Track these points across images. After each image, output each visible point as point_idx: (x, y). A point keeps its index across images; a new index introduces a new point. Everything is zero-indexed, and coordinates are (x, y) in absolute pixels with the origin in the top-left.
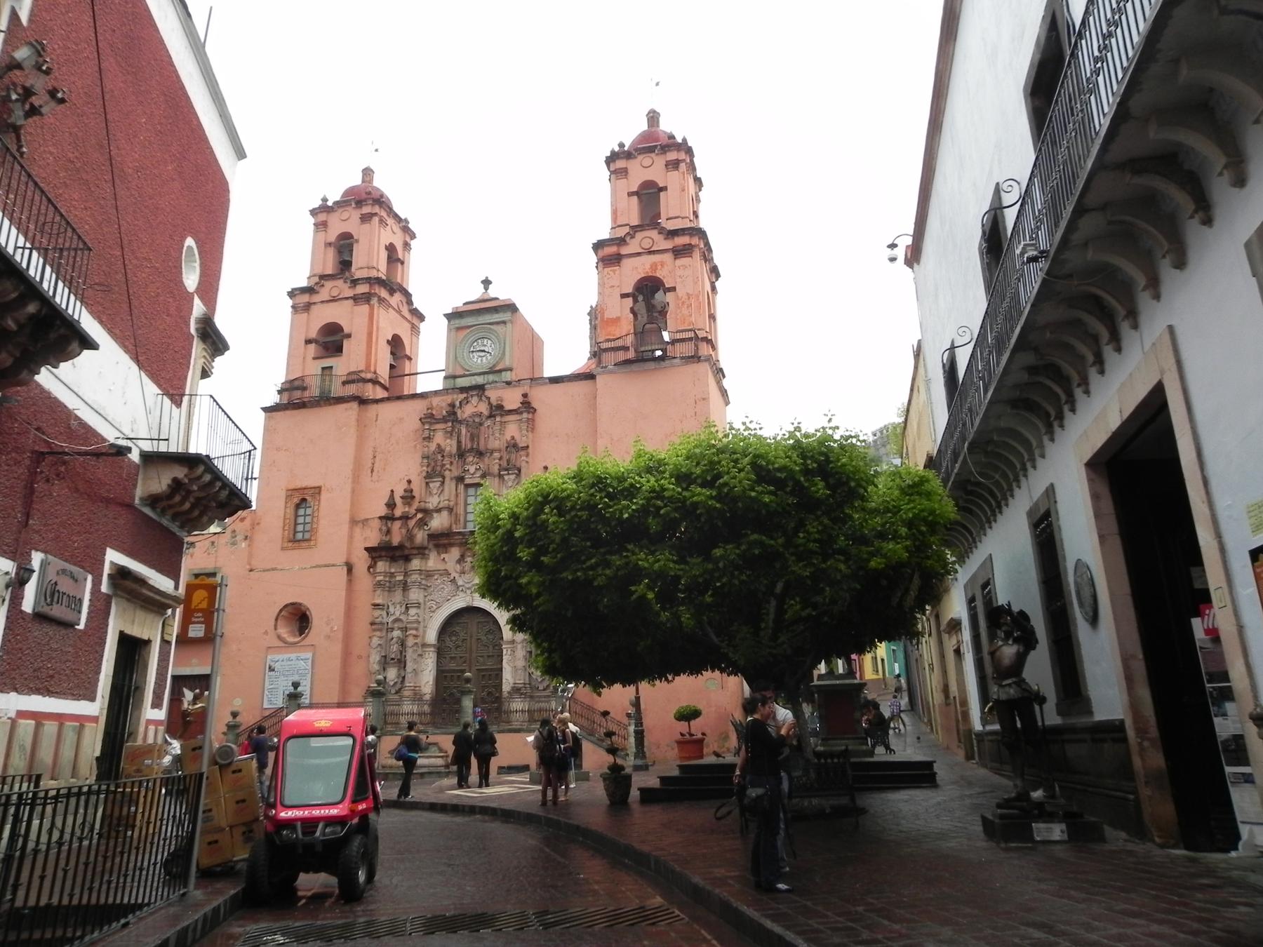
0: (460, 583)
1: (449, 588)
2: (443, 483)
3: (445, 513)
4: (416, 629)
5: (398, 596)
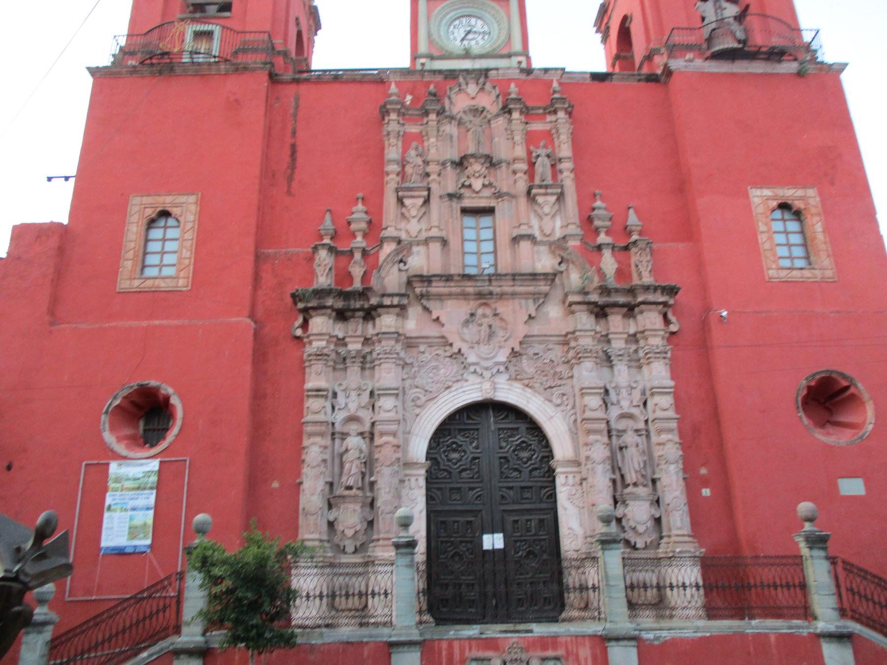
0: (472, 358)
1: (448, 369)
2: (427, 201)
3: (435, 247)
4: (394, 434)
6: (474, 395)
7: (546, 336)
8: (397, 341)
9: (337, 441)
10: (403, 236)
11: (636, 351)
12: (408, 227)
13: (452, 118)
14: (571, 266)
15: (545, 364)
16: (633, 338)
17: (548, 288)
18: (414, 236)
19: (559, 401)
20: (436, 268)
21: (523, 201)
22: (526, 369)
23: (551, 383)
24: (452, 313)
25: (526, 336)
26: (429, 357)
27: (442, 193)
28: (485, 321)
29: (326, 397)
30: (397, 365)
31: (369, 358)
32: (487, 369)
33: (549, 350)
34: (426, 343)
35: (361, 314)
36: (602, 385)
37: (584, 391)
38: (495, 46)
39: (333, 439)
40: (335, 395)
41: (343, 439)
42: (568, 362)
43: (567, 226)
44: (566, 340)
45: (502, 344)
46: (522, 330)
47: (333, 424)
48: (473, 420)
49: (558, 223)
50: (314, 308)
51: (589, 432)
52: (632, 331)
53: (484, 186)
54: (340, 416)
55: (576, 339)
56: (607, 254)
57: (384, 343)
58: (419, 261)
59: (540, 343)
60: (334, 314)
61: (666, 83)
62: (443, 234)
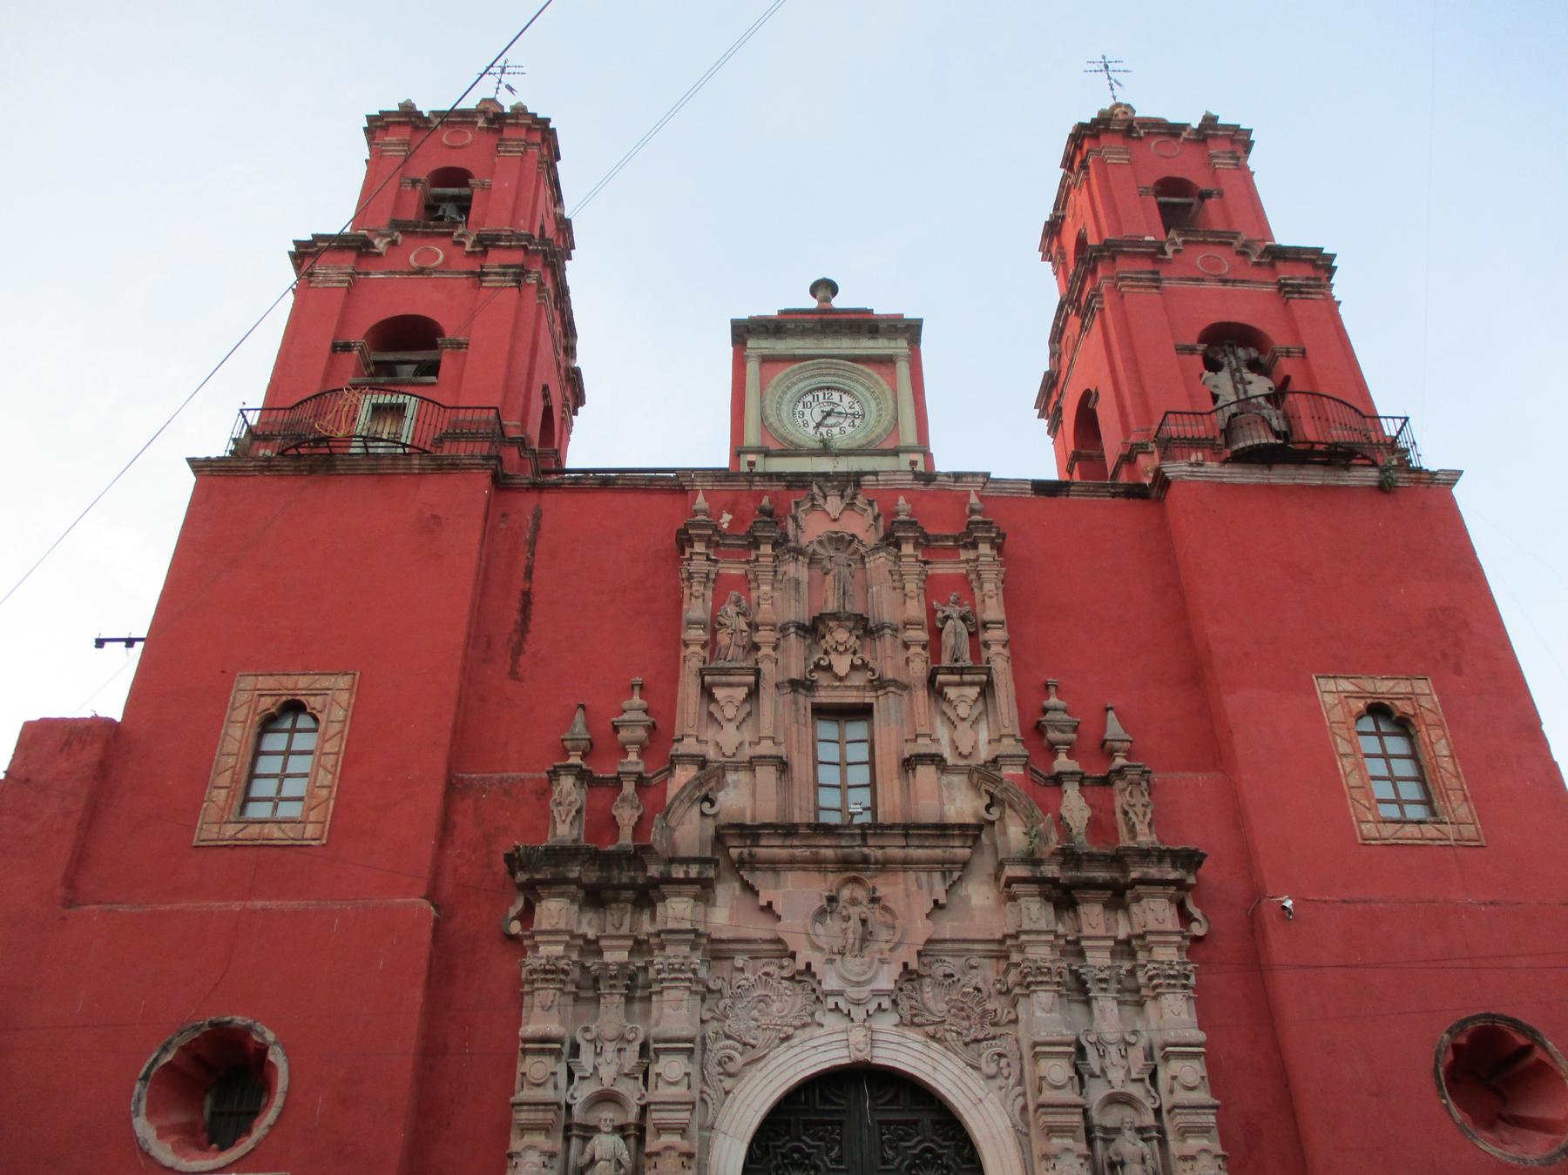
0: (831, 982)
1: (787, 1003)
2: (753, 693)
3: (767, 774)
4: (683, 1131)
5: (611, 1015)
6: (835, 1054)
7: (965, 941)
8: (694, 946)
9: (575, 1142)
10: (711, 753)
11: (1132, 973)
12: (720, 737)
13: (799, 552)
14: (1008, 811)
15: (965, 994)
16: (1125, 948)
17: (968, 851)
18: (729, 753)
19: (992, 1069)
20: (768, 811)
21: (921, 694)
22: (931, 1005)
23: (976, 1033)
24: (797, 895)
25: (929, 941)
26: (752, 978)
27: (780, 679)
28: (855, 911)
29: (557, 1054)
30: (692, 992)
31: (641, 979)
32: (858, 1003)
33: (972, 967)
34: (744, 952)
35: (629, 894)
36: (1073, 1038)
37: (1038, 1049)
38: (873, 436)
39: (567, 1139)
40: (575, 1050)
41: (586, 1140)
42: (1008, 991)
43: (999, 740)
44: (1002, 949)
45: (887, 955)
46: (921, 930)
47: (569, 1107)
48: (835, 1104)
49: (984, 734)
50: (546, 883)
51: (1051, 1131)
52: (1122, 935)
53: (853, 667)
54: (584, 1091)
55: (1021, 949)
56: (1072, 791)
57: (669, 950)
58: (739, 798)
59: (956, 954)
60: (581, 894)
61: (1160, 500)
62: (781, 751)
